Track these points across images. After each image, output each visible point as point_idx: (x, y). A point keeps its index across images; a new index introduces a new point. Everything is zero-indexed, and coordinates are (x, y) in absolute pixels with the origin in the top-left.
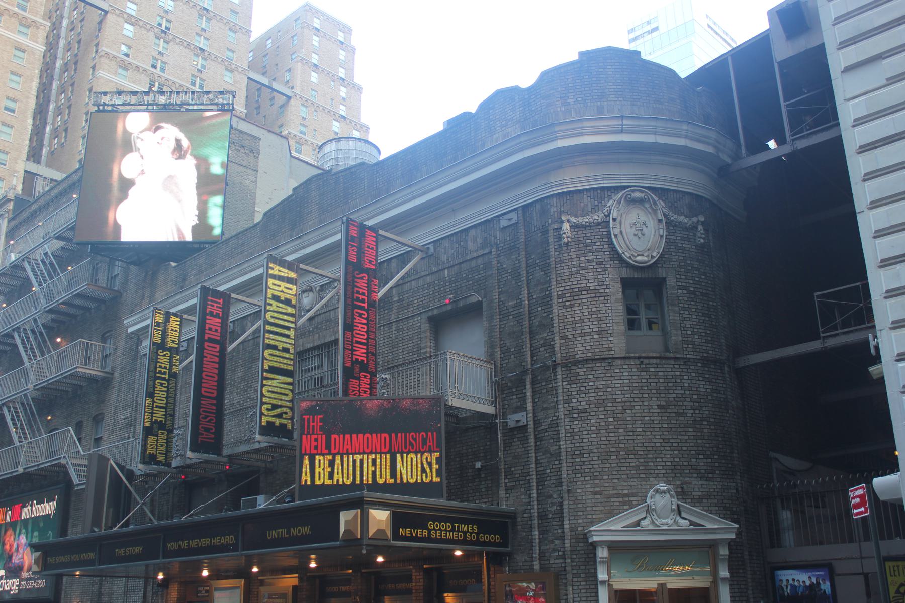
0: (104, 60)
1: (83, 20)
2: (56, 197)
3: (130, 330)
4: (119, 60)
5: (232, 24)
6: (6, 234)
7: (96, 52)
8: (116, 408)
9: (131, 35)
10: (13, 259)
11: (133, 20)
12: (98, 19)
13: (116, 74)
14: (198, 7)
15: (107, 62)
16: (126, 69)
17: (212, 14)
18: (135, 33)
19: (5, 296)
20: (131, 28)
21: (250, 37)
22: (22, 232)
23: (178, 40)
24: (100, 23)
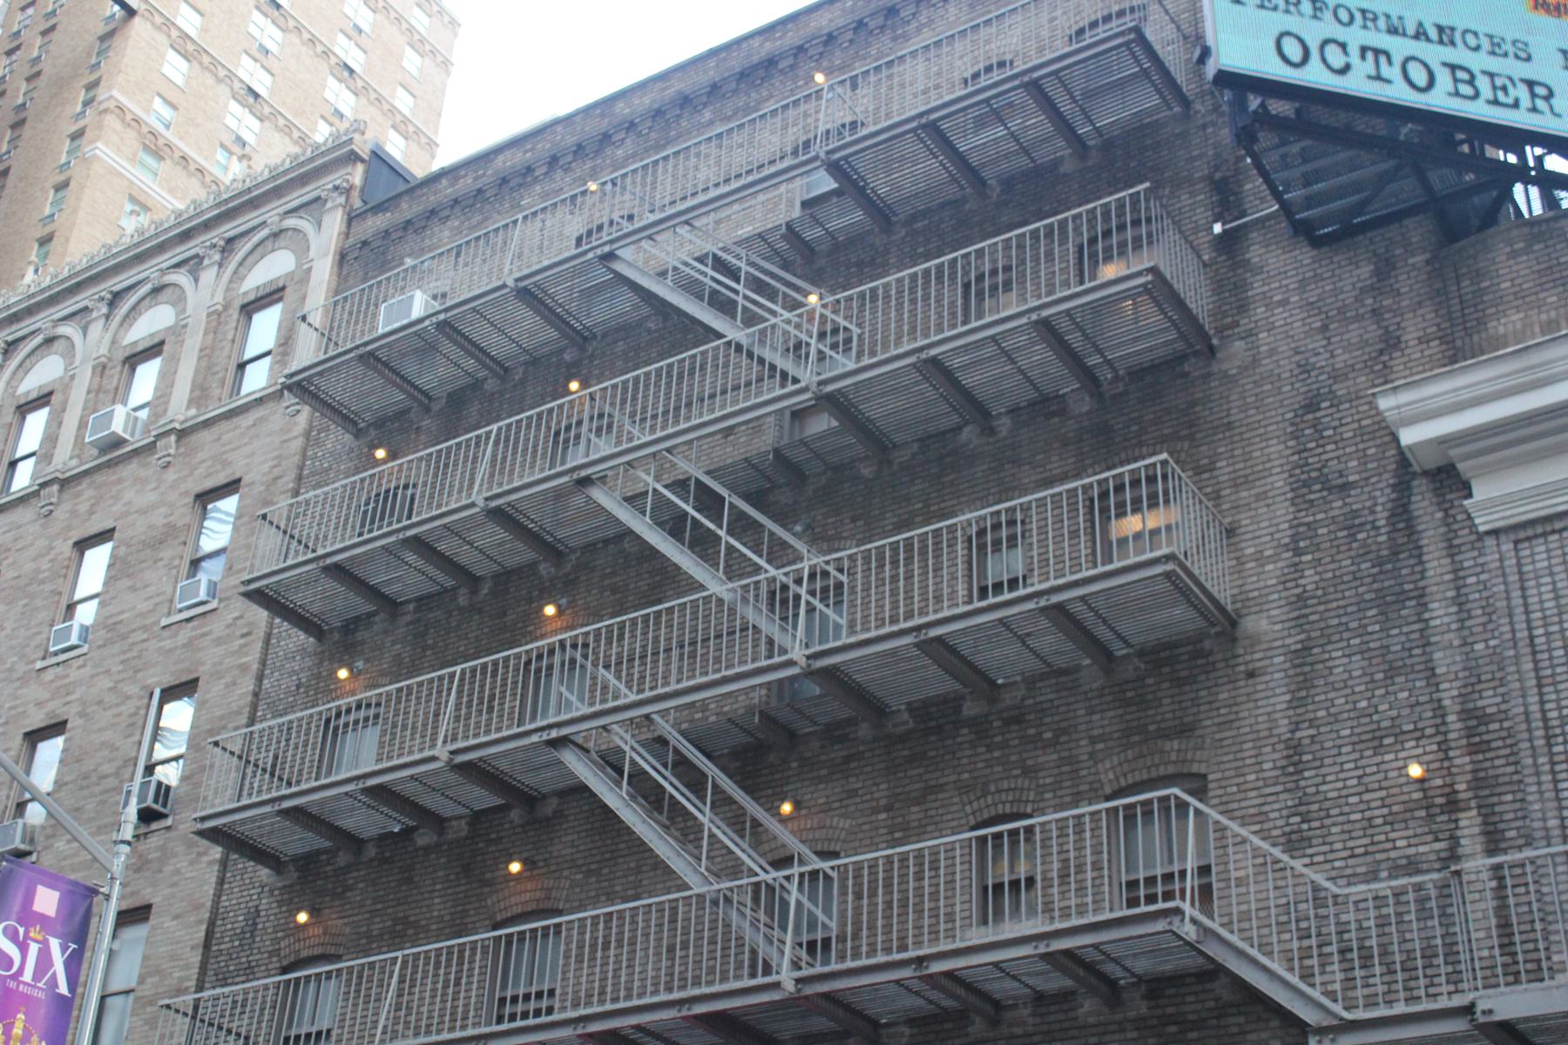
0: (111, 121)
1: (53, 28)
2: (658, 113)
3: (1408, 437)
4: (145, 130)
5: (399, 118)
6: (342, 258)
7: (86, 104)
8: (1295, 748)
9: (179, 81)
10: (417, 312)
11: (190, 47)
12: (102, 29)
13: (133, 160)
14: (333, 60)
15: (118, 125)
16: (157, 154)
17: (360, 84)
18: (188, 78)
19: (358, 434)
20: (183, 65)
21: (433, 156)
22: (443, 236)
23: (281, 122)
24: (111, 34)
